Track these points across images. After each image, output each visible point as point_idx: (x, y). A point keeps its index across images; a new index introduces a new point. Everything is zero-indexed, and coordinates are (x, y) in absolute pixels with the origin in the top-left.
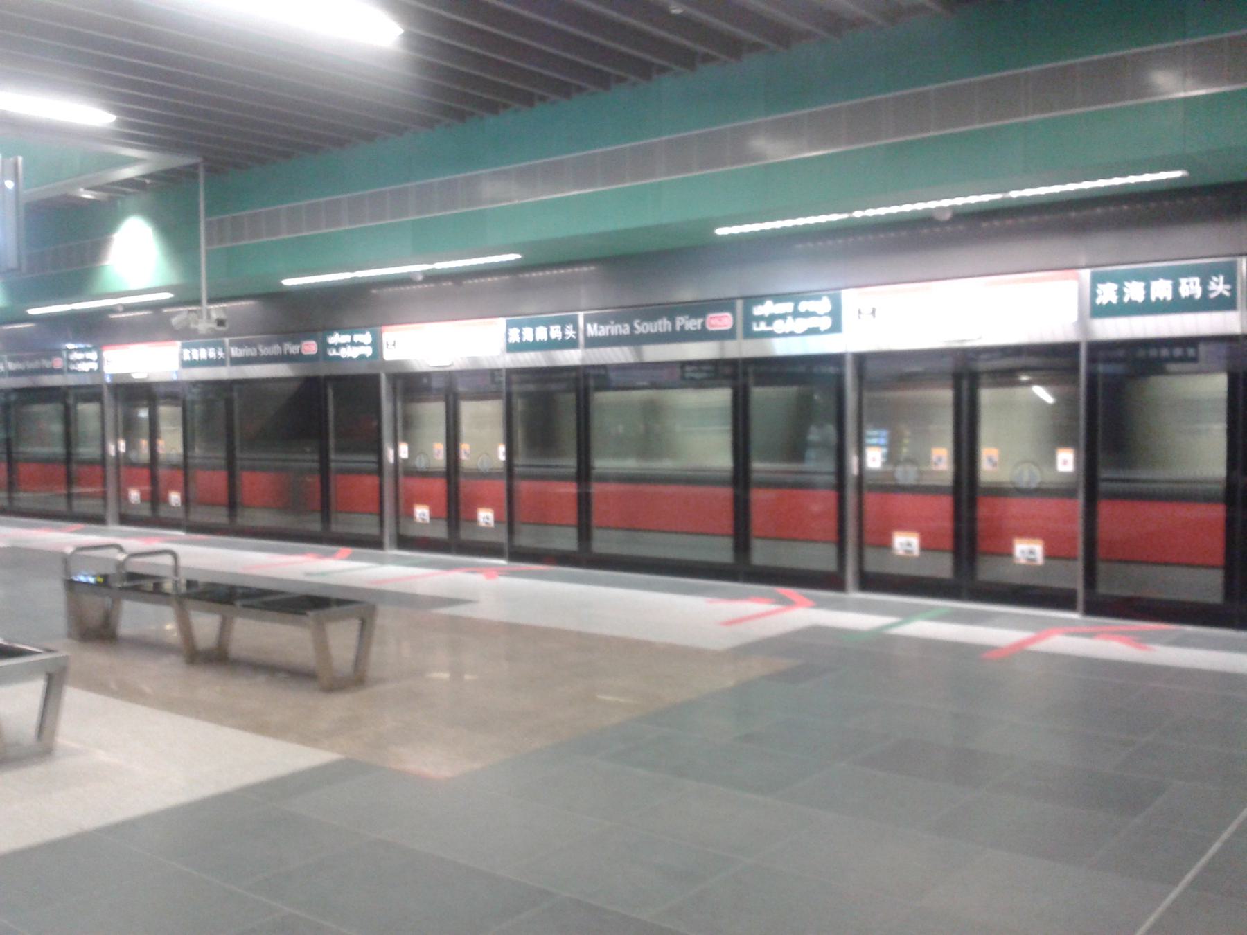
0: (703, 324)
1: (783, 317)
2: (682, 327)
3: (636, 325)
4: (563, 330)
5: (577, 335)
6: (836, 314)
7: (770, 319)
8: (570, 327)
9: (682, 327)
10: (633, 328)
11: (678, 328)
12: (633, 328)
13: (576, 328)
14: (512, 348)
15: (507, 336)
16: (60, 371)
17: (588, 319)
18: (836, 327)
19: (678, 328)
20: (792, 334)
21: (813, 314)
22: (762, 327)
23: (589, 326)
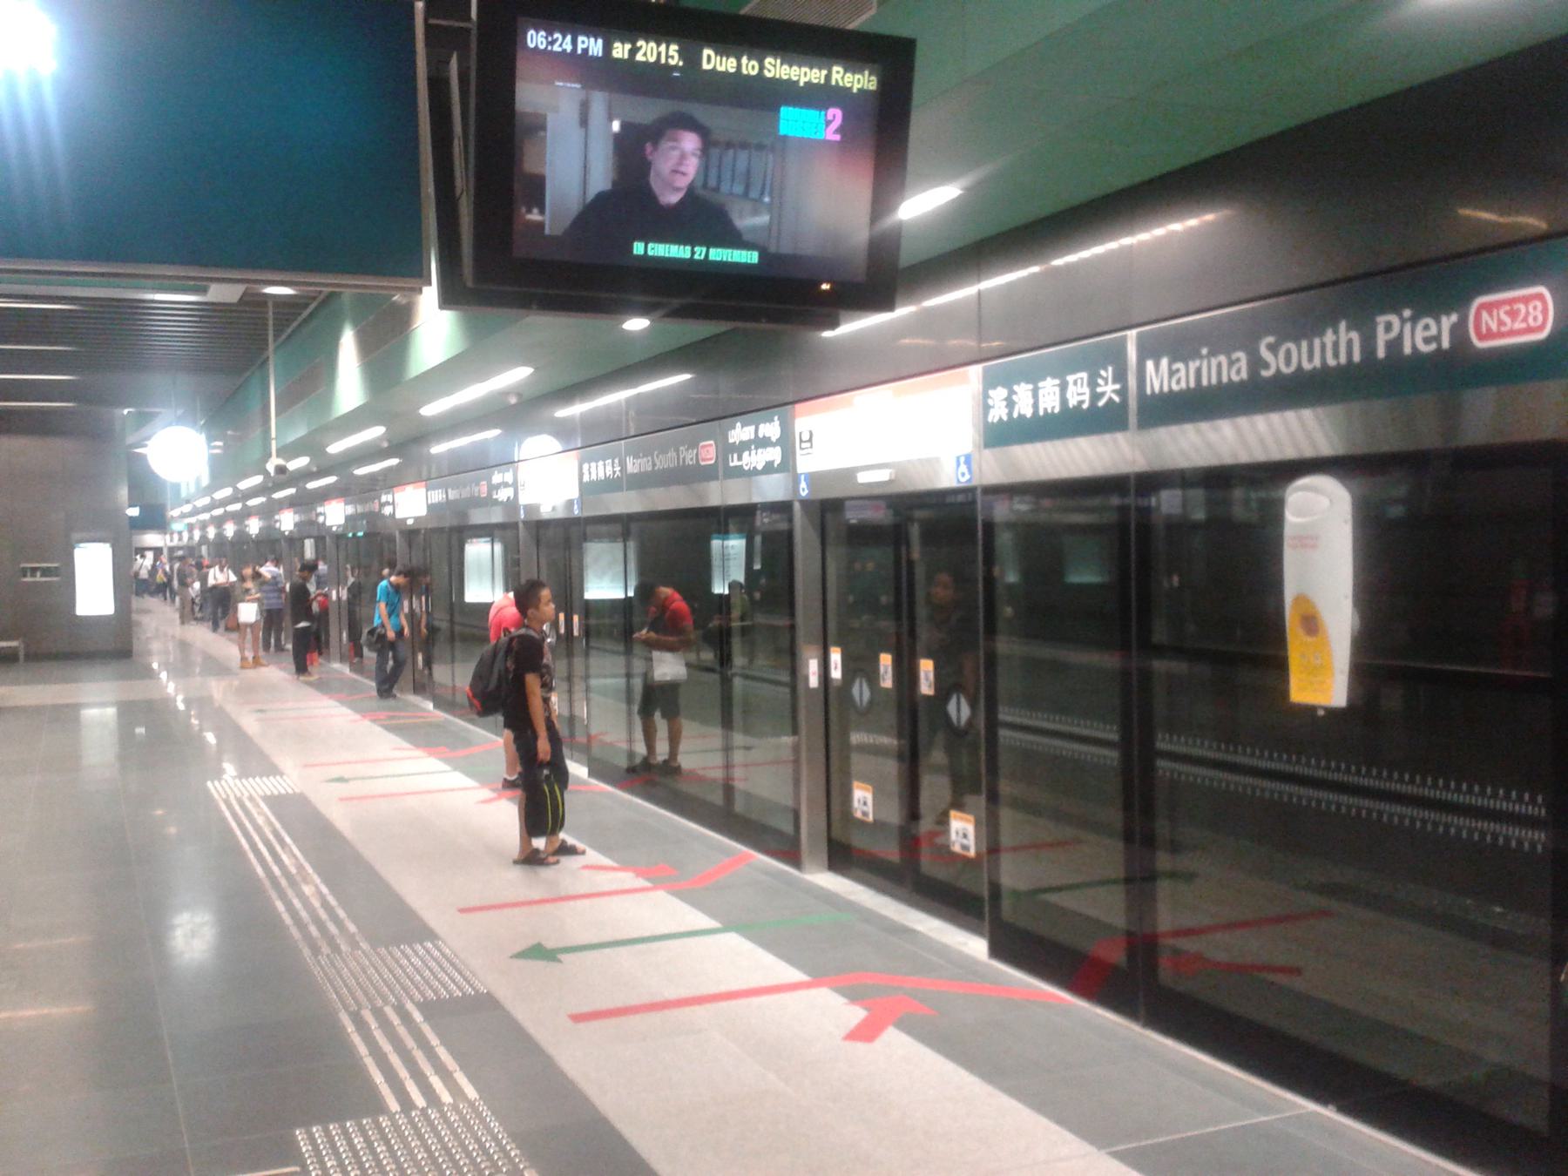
0: (1459, 331)
2: (1395, 345)
3: (1265, 354)
4: (1093, 384)
5: (1123, 393)
8: (1108, 373)
9: (1395, 345)
10: (1256, 363)
11: (1381, 353)
12: (1256, 363)
13: (1120, 376)
14: (1000, 435)
15: (986, 408)
16: (709, 474)
17: (1148, 350)
19: (1381, 353)
23: (1150, 365)
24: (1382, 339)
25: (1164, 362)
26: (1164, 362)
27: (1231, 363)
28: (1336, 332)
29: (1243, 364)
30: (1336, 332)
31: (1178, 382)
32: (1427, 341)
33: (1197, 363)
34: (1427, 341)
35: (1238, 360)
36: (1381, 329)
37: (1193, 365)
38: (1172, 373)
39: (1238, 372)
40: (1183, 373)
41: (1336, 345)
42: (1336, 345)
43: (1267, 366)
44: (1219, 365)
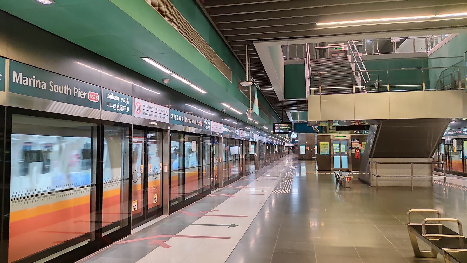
1: (116, 102)
2: (77, 94)
6: (130, 106)
7: (113, 102)
9: (77, 94)
18: (130, 113)
20: (118, 111)
21: (123, 104)
22: (109, 106)
23: (15, 73)
24: (75, 92)
25: (20, 75)
26: (20, 75)
27: (42, 84)
28: (66, 87)
29: (45, 85)
30: (66, 87)
31: (25, 82)
32: (82, 96)
33: (32, 79)
34: (82, 96)
35: (44, 84)
36: (75, 90)
37: (30, 80)
38: (23, 79)
39: (44, 87)
40: (27, 80)
41: (66, 89)
42: (66, 89)
43: (51, 89)
44: (38, 82)
